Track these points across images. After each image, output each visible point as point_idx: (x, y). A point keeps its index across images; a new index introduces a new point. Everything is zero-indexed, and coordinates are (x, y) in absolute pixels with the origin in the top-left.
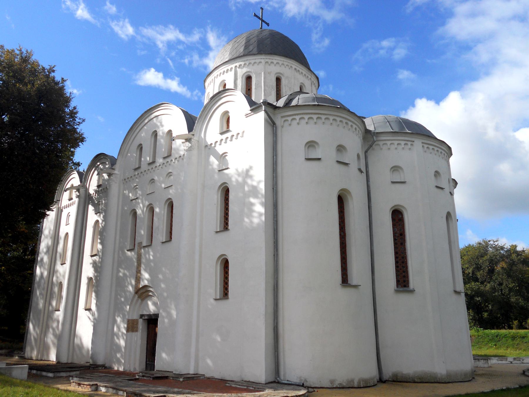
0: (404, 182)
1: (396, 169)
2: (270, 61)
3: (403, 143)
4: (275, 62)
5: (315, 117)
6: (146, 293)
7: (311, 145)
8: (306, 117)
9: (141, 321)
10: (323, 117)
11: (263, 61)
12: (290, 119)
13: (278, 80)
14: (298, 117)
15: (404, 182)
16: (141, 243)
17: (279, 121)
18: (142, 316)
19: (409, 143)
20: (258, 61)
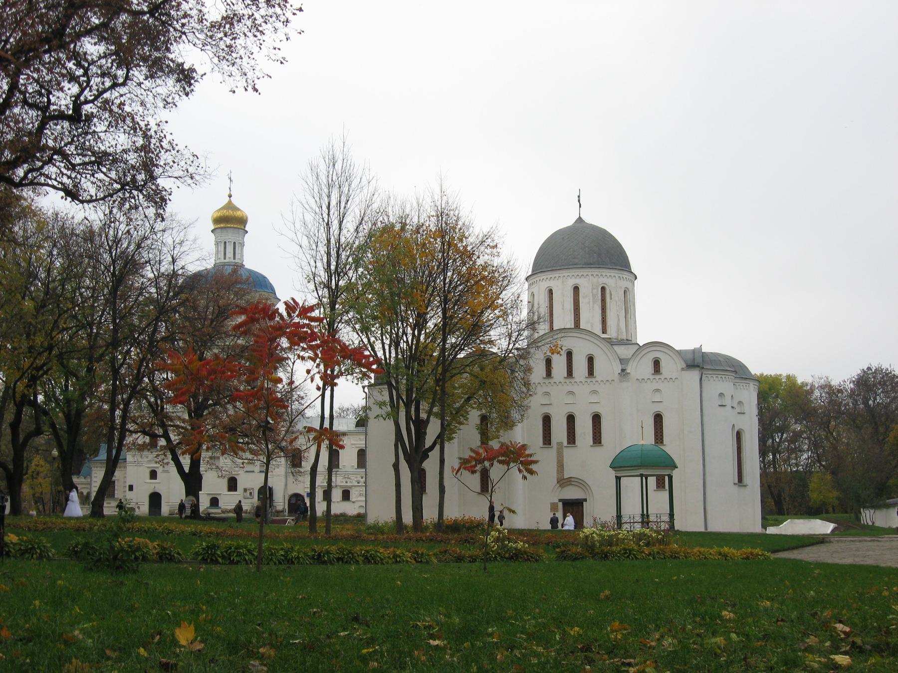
0: (744, 413)
1: (740, 403)
2: (621, 276)
3: (744, 385)
4: (625, 277)
5: (723, 376)
6: (569, 483)
7: (721, 395)
8: (720, 376)
9: (560, 504)
10: (727, 377)
11: (616, 275)
12: (710, 376)
13: (625, 292)
14: (714, 376)
15: (744, 413)
16: (562, 443)
17: (704, 376)
18: (560, 500)
19: (747, 385)
20: (612, 275)
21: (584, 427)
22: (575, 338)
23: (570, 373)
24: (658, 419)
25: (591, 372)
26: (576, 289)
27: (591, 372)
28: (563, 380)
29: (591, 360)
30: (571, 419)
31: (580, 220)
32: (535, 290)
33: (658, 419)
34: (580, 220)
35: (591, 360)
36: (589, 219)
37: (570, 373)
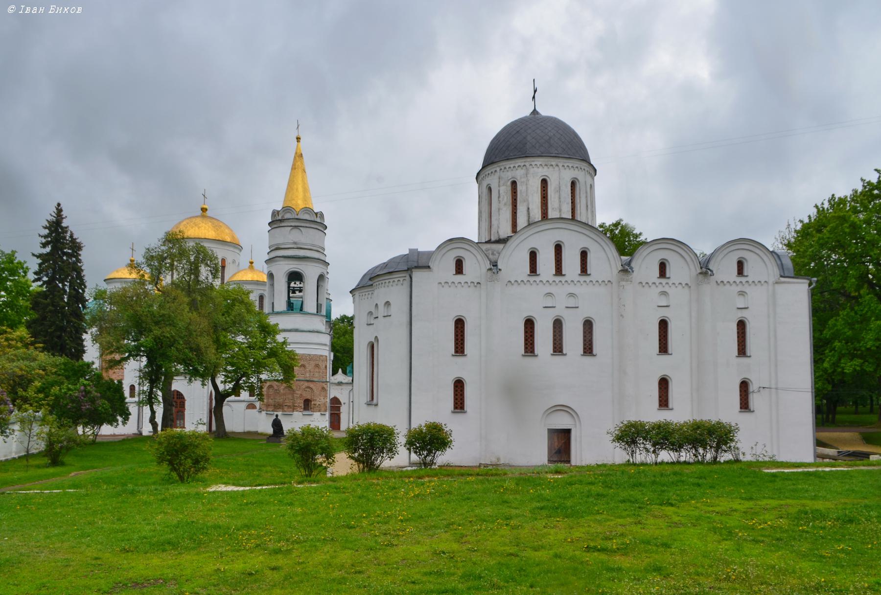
21: (573, 338)
22: (562, 230)
23: (559, 271)
24: (663, 325)
25: (584, 270)
26: (544, 182)
27: (584, 270)
28: (552, 278)
29: (584, 255)
30: (558, 325)
31: (535, 112)
32: (493, 181)
33: (663, 325)
34: (535, 112)
35: (584, 255)
36: (544, 112)
37: (559, 271)
